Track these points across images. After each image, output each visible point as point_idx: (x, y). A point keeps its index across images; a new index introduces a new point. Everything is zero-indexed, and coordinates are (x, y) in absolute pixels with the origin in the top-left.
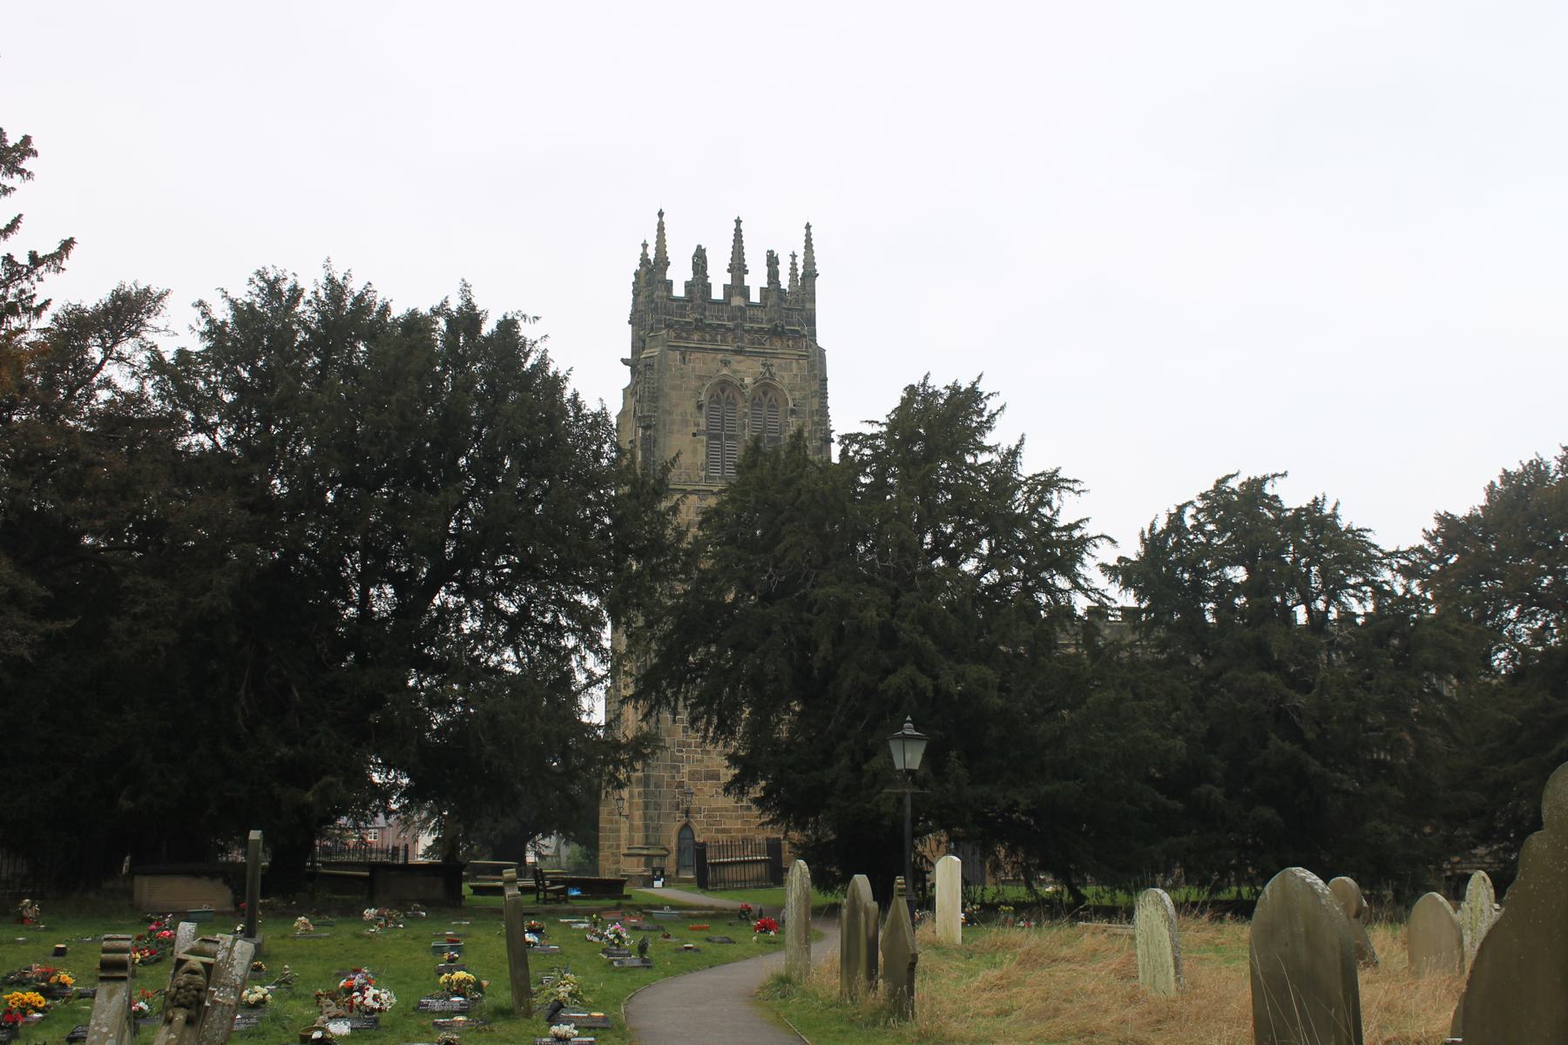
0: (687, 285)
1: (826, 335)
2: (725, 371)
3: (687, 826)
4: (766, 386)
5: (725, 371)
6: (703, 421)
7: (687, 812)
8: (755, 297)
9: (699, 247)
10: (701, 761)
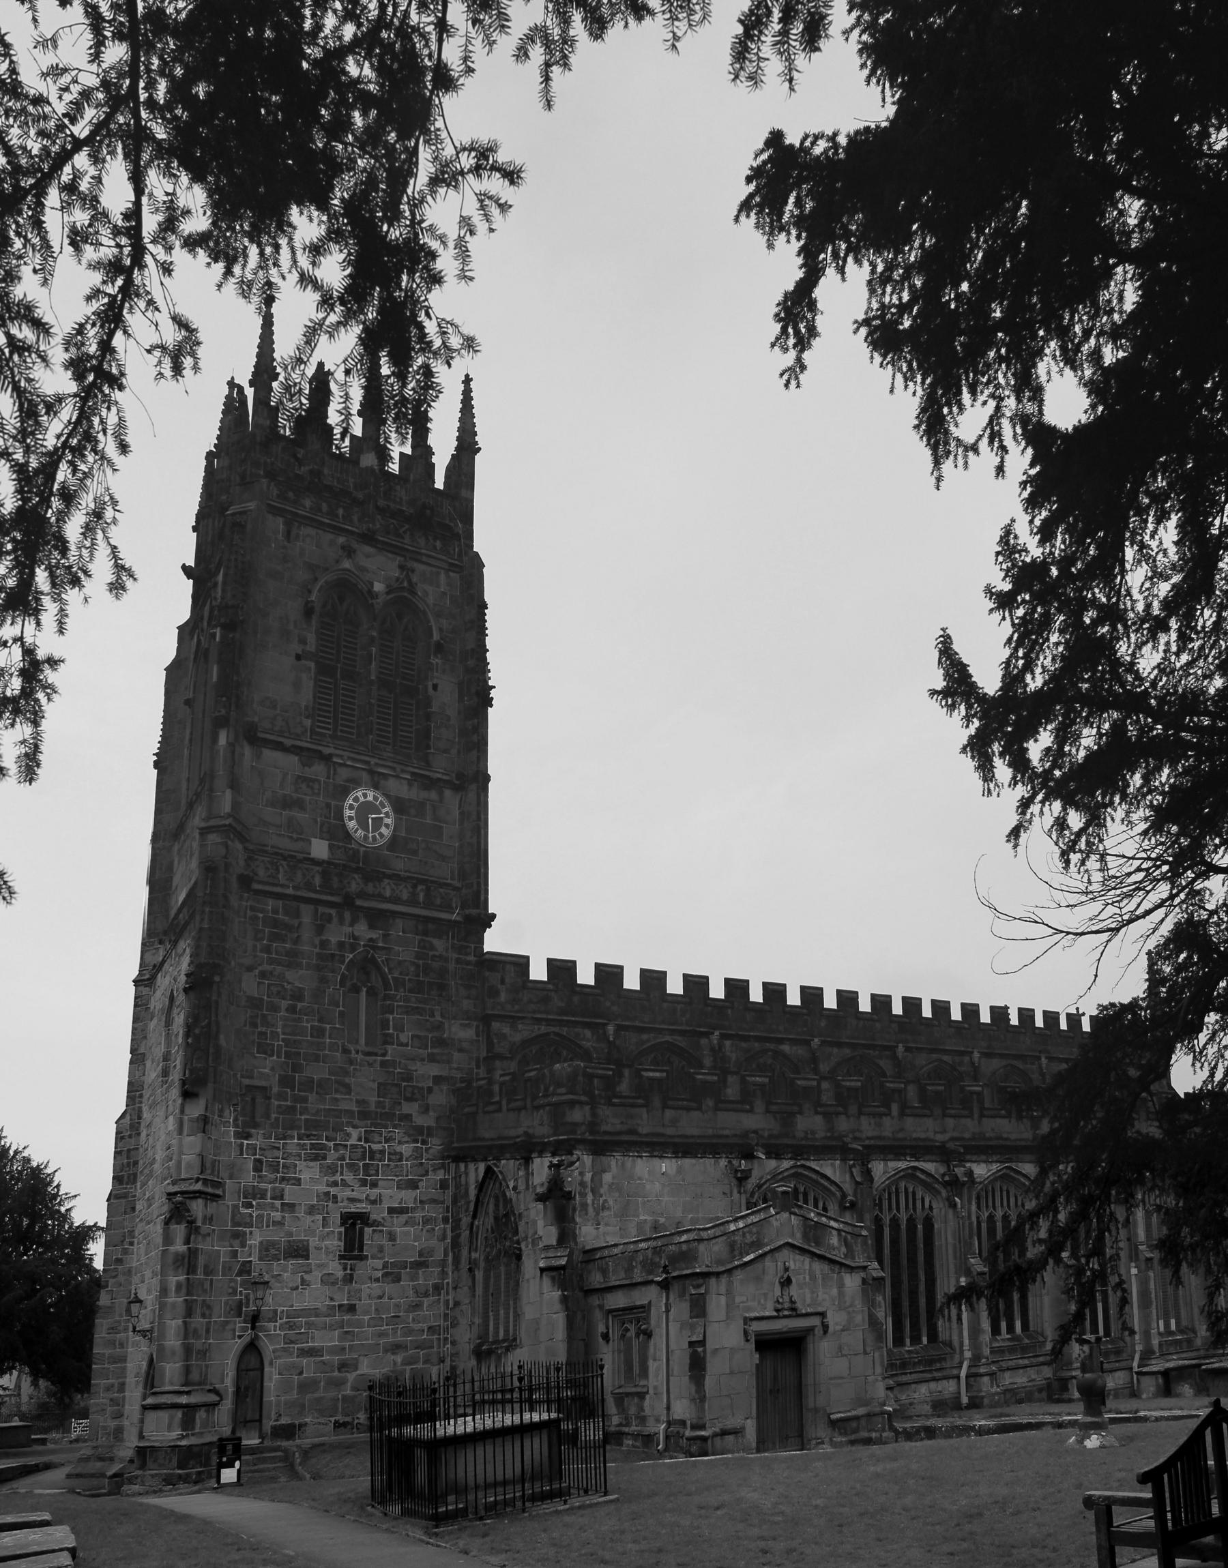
1: (486, 539)
3: (252, 1348)
4: (403, 600)
5: (347, 564)
6: (311, 638)
7: (255, 1319)
10: (280, 1223)
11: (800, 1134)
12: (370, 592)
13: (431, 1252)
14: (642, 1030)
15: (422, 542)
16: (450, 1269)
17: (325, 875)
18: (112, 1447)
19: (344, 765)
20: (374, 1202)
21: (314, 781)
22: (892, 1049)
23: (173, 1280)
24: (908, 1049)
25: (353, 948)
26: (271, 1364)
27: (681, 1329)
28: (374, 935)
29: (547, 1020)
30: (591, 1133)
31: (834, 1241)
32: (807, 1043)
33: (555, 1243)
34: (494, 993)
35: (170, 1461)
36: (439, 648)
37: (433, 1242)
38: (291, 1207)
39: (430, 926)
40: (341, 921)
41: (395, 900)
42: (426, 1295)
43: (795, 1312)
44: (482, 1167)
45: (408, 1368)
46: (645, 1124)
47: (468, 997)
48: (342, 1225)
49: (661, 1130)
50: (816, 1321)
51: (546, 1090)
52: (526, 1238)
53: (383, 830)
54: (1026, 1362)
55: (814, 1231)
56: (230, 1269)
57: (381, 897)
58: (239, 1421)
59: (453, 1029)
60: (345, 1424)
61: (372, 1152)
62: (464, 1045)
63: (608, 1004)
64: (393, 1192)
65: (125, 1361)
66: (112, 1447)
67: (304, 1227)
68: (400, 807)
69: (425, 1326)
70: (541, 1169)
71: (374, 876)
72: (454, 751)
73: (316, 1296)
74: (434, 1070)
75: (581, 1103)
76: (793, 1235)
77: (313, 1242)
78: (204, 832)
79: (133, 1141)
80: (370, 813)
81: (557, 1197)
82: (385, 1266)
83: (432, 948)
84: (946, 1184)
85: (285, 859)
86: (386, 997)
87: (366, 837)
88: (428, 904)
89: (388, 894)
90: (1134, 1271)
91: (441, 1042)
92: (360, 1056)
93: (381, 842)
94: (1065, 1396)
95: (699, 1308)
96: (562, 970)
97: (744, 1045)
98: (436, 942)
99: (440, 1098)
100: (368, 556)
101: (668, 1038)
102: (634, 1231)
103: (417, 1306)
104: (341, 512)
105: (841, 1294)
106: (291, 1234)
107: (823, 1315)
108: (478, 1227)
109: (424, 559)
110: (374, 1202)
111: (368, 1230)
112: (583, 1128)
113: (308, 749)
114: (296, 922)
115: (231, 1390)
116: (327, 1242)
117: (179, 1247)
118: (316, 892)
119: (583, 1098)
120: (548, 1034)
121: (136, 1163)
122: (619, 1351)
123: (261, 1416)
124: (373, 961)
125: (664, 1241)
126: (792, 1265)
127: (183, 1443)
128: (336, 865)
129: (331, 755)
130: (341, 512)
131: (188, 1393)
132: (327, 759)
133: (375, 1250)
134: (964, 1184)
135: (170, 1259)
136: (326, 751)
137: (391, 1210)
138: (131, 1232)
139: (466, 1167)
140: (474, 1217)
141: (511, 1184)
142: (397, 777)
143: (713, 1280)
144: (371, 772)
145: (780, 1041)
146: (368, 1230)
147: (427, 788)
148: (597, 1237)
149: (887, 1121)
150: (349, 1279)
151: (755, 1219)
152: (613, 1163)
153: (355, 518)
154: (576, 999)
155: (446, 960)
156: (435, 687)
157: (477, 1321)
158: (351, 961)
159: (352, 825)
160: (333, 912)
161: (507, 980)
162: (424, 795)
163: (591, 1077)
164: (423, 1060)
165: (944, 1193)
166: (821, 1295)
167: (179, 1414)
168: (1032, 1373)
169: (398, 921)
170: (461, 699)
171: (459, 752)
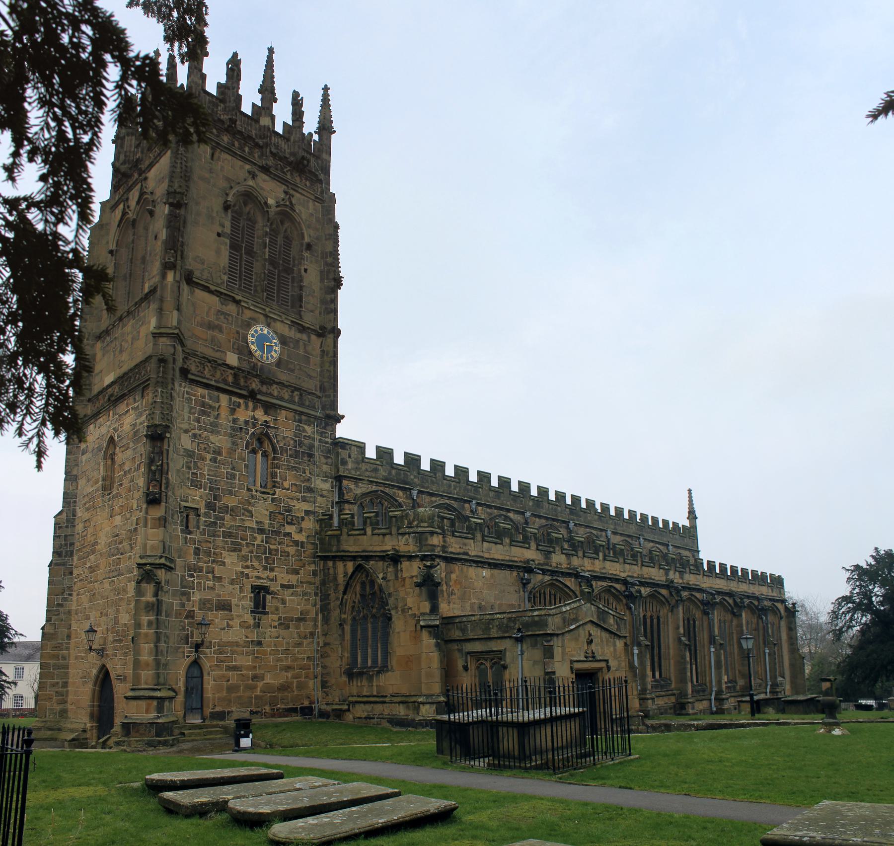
0: (220, 86)
2: (251, 183)
3: (196, 663)
4: (286, 214)
5: (251, 183)
6: (228, 224)
7: (198, 647)
8: (279, 128)
9: (235, 55)
10: (213, 588)
11: (554, 565)
12: (266, 203)
13: (308, 612)
14: (431, 495)
15: (298, 179)
16: (319, 624)
17: (235, 376)
18: (59, 721)
19: (249, 308)
20: (272, 580)
21: (229, 315)
22: (567, 523)
23: (145, 619)
24: (575, 525)
25: (254, 426)
26: (209, 674)
27: (534, 665)
28: (267, 418)
29: (376, 482)
30: (444, 552)
31: (612, 621)
32: (523, 513)
33: (428, 611)
34: (344, 463)
35: (150, 731)
36: (309, 247)
37: (309, 607)
38: (220, 579)
39: (303, 417)
40: (247, 408)
41: (281, 399)
42: (305, 638)
43: (594, 659)
44: (350, 566)
45: (295, 680)
46: (474, 548)
47: (326, 464)
48: (252, 592)
49: (482, 554)
50: (603, 665)
51: (410, 523)
52: (396, 608)
53: (273, 353)
54: (663, 693)
55: (602, 614)
56: (180, 614)
57: (271, 395)
58: (189, 709)
59: (317, 482)
60: (257, 713)
61: (270, 551)
62: (325, 493)
63: (412, 477)
64: (284, 575)
65: (68, 668)
66: (59, 721)
67: (227, 591)
68: (284, 341)
69: (305, 656)
70: (412, 570)
71: (267, 381)
72: (317, 312)
73: (236, 634)
74: (306, 506)
75: (437, 533)
76: (592, 616)
77: (234, 601)
78: (156, 336)
79: (69, 529)
80: (265, 342)
81: (429, 586)
82: (280, 619)
83: (304, 431)
84: (626, 597)
85: (209, 362)
86: (274, 458)
87: (262, 356)
88: (301, 404)
89: (276, 393)
90: (713, 650)
91: (310, 490)
92: (258, 494)
93: (271, 361)
94: (684, 712)
95: (549, 653)
96: (385, 454)
97: (488, 510)
98: (306, 427)
99: (309, 524)
100: (264, 181)
101: (446, 501)
102: (469, 608)
103: (300, 644)
104: (247, 149)
105: (615, 650)
106: (220, 596)
107: (607, 661)
108: (347, 600)
109: (300, 190)
110: (272, 580)
111: (268, 597)
112: (439, 549)
113: (226, 294)
114: (217, 405)
115: (183, 689)
116: (243, 603)
117: (149, 598)
118: (230, 386)
119: (439, 531)
120: (377, 491)
121: (72, 544)
122: (475, 676)
123: (202, 705)
124: (267, 435)
125: (519, 614)
126: (591, 632)
127: (159, 721)
128: (243, 371)
129: (240, 301)
130: (247, 149)
131: (160, 690)
132: (237, 302)
133: (273, 609)
134: (636, 597)
135: (142, 606)
136: (238, 298)
137: (283, 586)
138: (70, 588)
139: (334, 564)
140: (345, 593)
141: (381, 576)
142: (282, 322)
143: (555, 638)
144: (266, 316)
145: (508, 511)
146: (268, 597)
147: (300, 332)
148: (449, 610)
149: (597, 562)
150: (257, 625)
151: (575, 605)
152: (456, 568)
153: (256, 155)
154: (394, 472)
155: (313, 439)
156: (306, 270)
157: (346, 655)
158: (253, 433)
159: (253, 347)
160: (241, 401)
161: (352, 456)
162: (299, 335)
163: (443, 518)
164: (298, 500)
165: (624, 601)
166: (606, 651)
167: (155, 703)
168: (666, 699)
169: (283, 411)
170: (322, 280)
171: (320, 313)
